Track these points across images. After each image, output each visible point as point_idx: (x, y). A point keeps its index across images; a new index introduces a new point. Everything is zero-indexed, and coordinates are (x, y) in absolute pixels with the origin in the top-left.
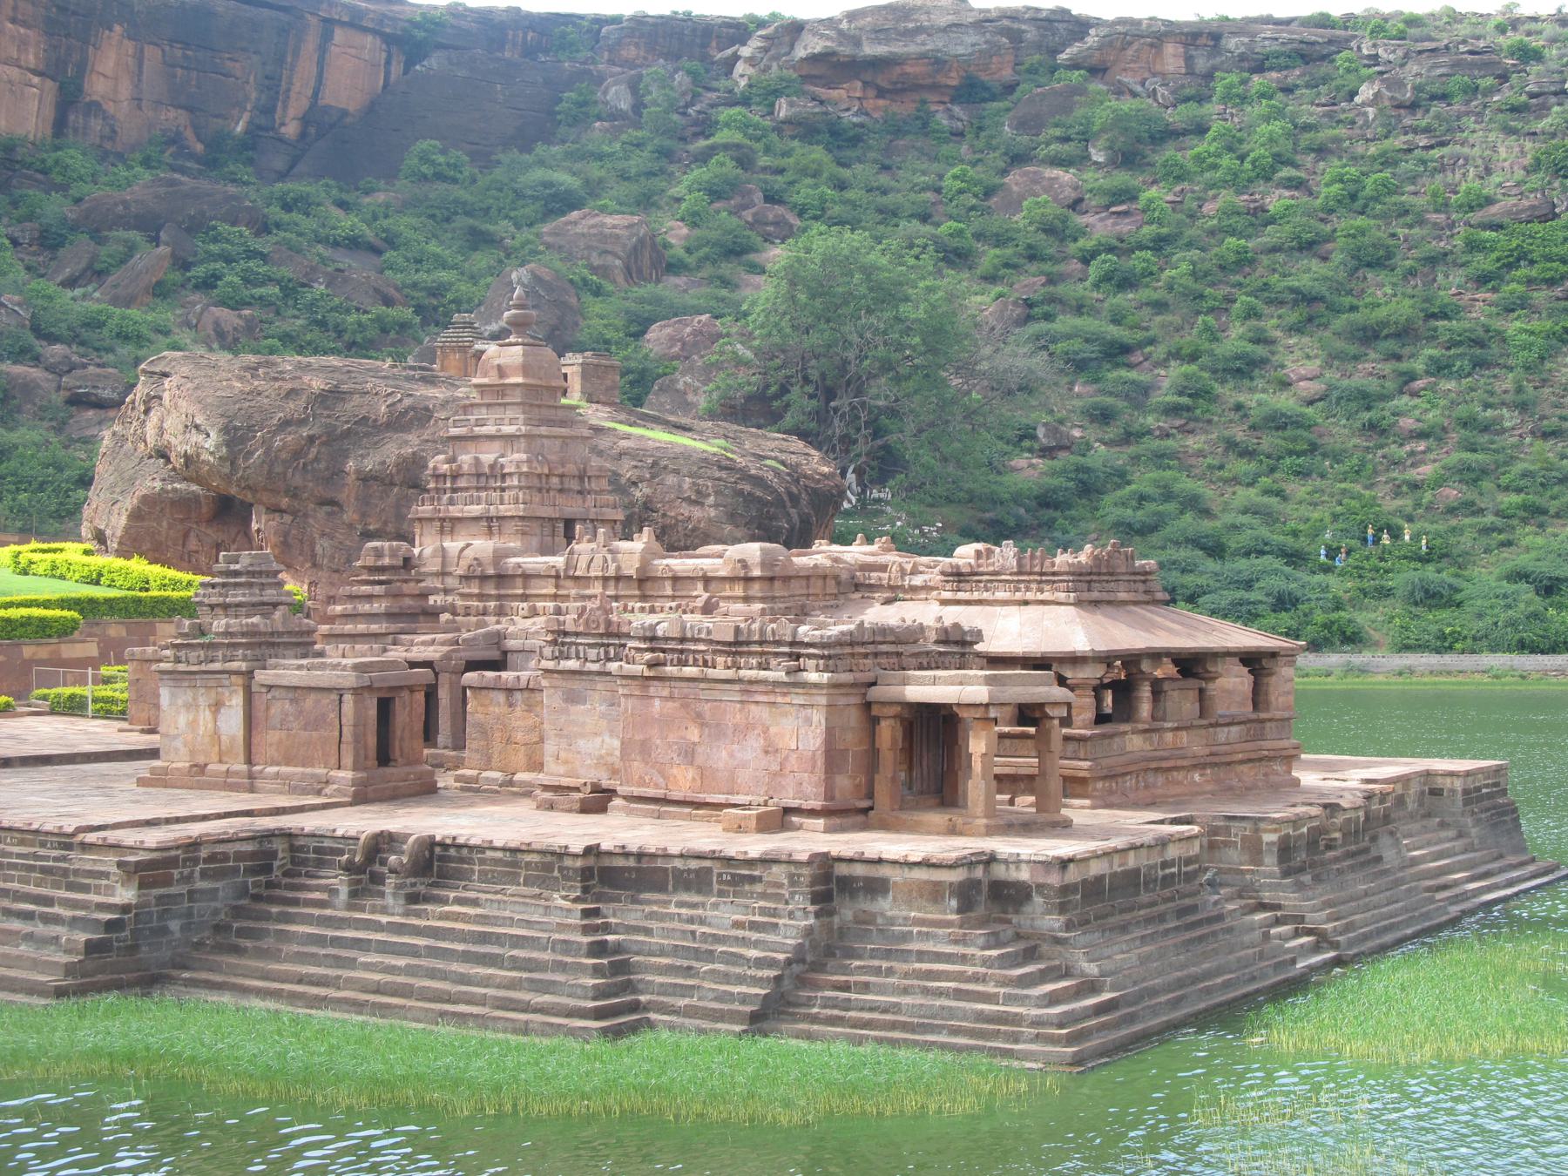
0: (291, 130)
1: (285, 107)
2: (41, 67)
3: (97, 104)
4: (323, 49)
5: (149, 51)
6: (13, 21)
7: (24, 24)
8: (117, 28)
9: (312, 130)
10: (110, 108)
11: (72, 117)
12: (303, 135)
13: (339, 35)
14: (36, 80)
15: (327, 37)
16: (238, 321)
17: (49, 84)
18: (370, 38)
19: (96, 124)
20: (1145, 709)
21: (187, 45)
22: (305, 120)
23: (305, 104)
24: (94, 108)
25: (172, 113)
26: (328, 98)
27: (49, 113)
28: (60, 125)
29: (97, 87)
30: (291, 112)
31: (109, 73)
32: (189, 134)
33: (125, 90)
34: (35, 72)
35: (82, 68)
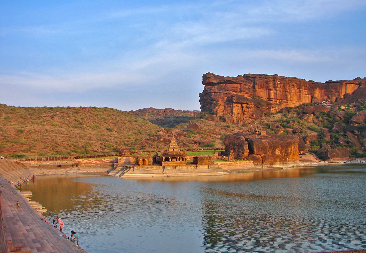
0: (342, 97)
1: (341, 94)
2: (308, 94)
3: (316, 97)
4: (346, 87)
5: (322, 90)
6: (304, 89)
7: (306, 90)
8: (318, 88)
9: (345, 97)
10: (318, 97)
11: (313, 99)
12: (344, 97)
13: (348, 85)
14: (308, 96)
15: (346, 85)
16: (319, 122)
17: (310, 96)
18: (353, 84)
19: (316, 100)
20: (170, 160)
21: (327, 89)
22: (344, 95)
23: (344, 94)
24: (316, 98)
25: (326, 97)
26: (347, 93)
27: (310, 99)
28: (312, 100)
29: (316, 95)
30: (342, 95)
31: (317, 93)
32: (328, 99)
33: (320, 95)
34: (307, 95)
35: (314, 94)
